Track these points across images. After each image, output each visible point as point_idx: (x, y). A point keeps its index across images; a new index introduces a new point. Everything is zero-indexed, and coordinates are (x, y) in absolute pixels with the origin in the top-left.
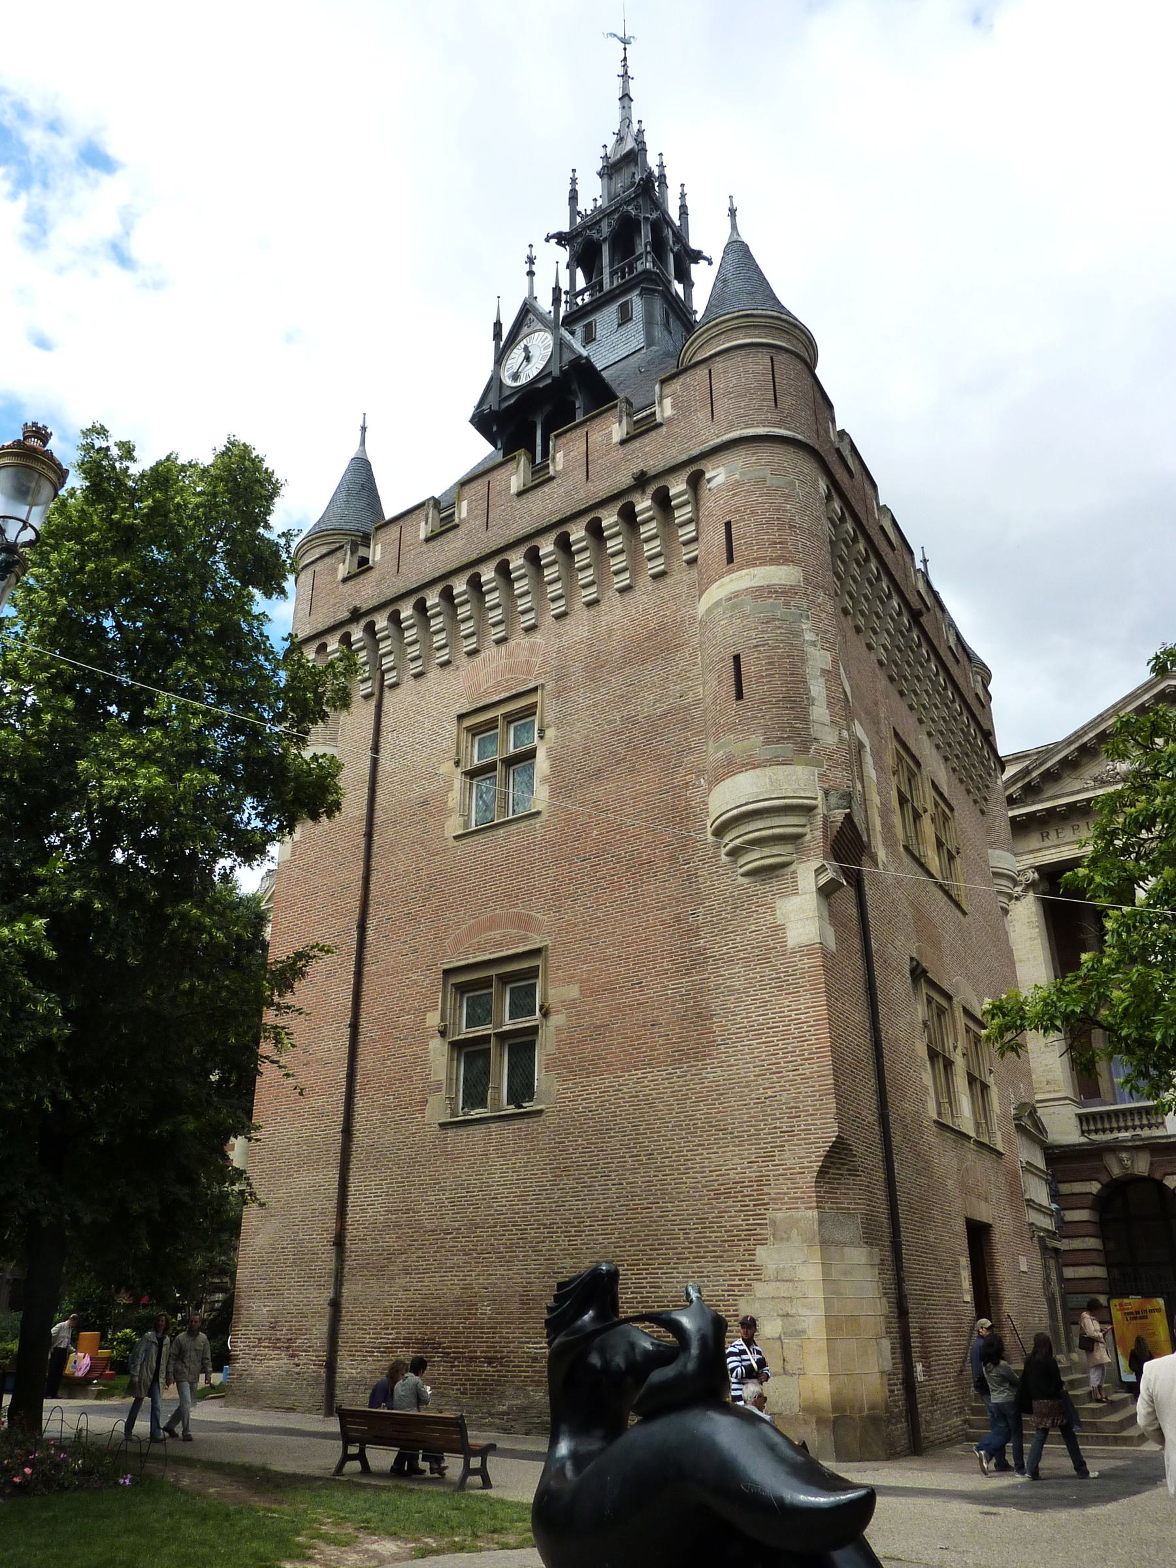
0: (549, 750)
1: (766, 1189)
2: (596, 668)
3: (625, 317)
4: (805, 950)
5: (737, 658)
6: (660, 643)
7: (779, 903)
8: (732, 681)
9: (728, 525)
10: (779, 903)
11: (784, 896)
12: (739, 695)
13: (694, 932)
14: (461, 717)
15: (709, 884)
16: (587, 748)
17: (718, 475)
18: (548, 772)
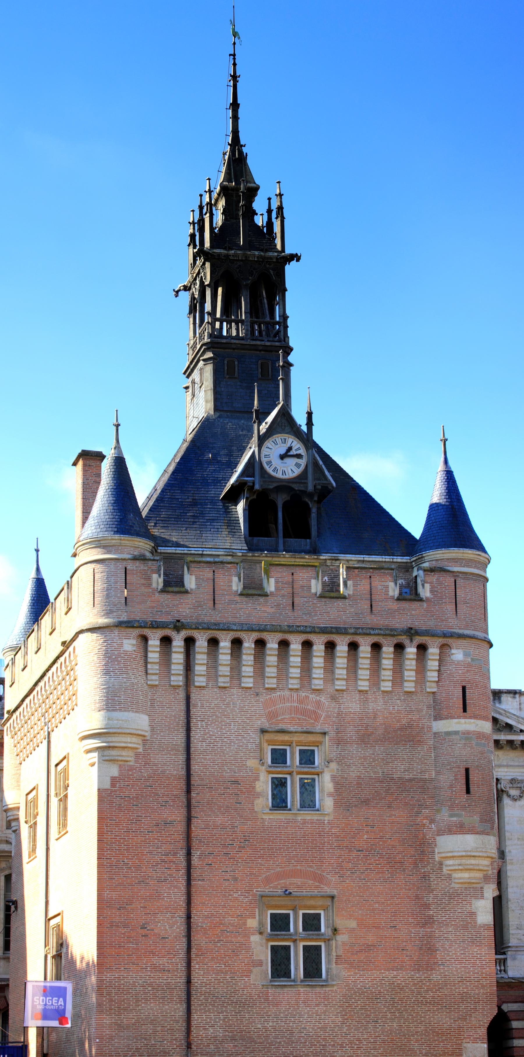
0: (333, 778)
1: (462, 1033)
4: (485, 926)
5: (467, 770)
6: (406, 735)
7: (474, 901)
8: (464, 781)
9: (464, 688)
10: (474, 901)
11: (476, 898)
12: (468, 791)
13: (427, 906)
14: (263, 731)
15: (435, 883)
16: (358, 784)
17: (458, 655)
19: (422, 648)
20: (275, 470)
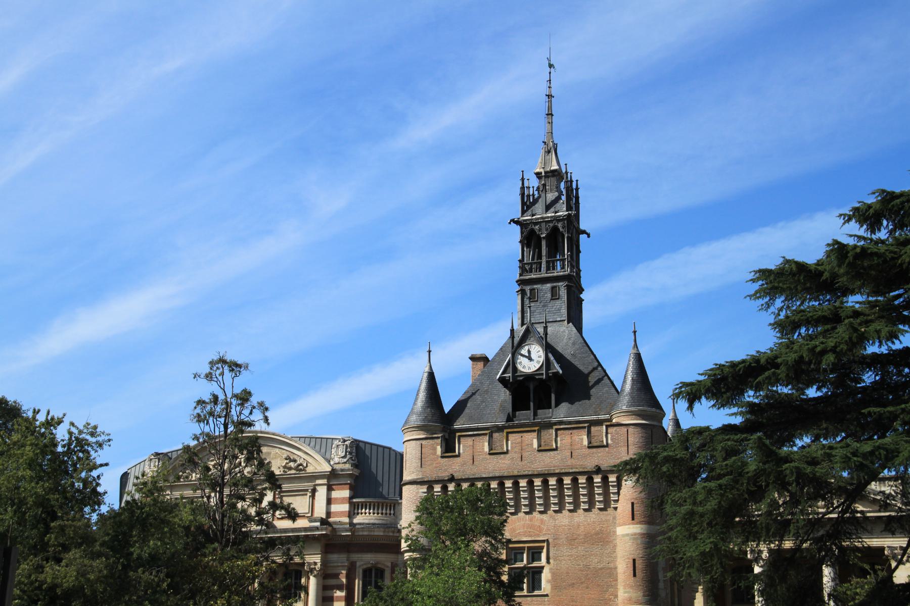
0: (551, 569)
2: (572, 540)
3: (555, 295)
12: (635, 575)
16: (568, 573)
18: (550, 578)
19: (605, 479)
20: (524, 367)
